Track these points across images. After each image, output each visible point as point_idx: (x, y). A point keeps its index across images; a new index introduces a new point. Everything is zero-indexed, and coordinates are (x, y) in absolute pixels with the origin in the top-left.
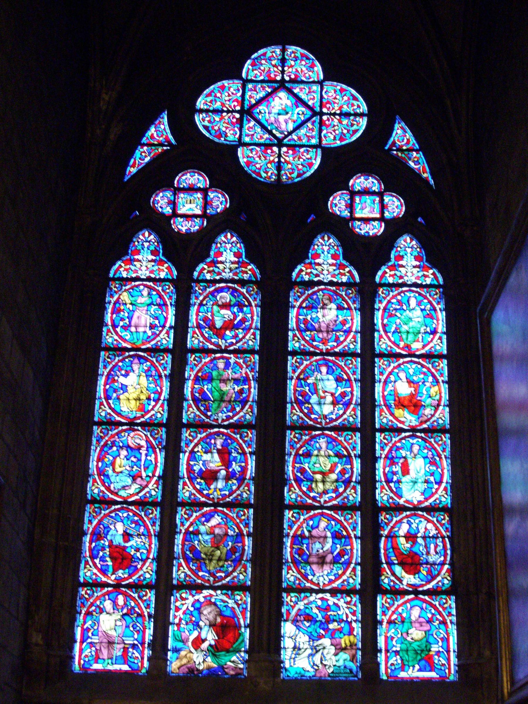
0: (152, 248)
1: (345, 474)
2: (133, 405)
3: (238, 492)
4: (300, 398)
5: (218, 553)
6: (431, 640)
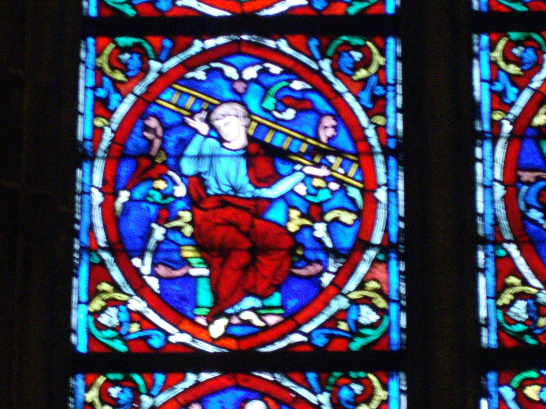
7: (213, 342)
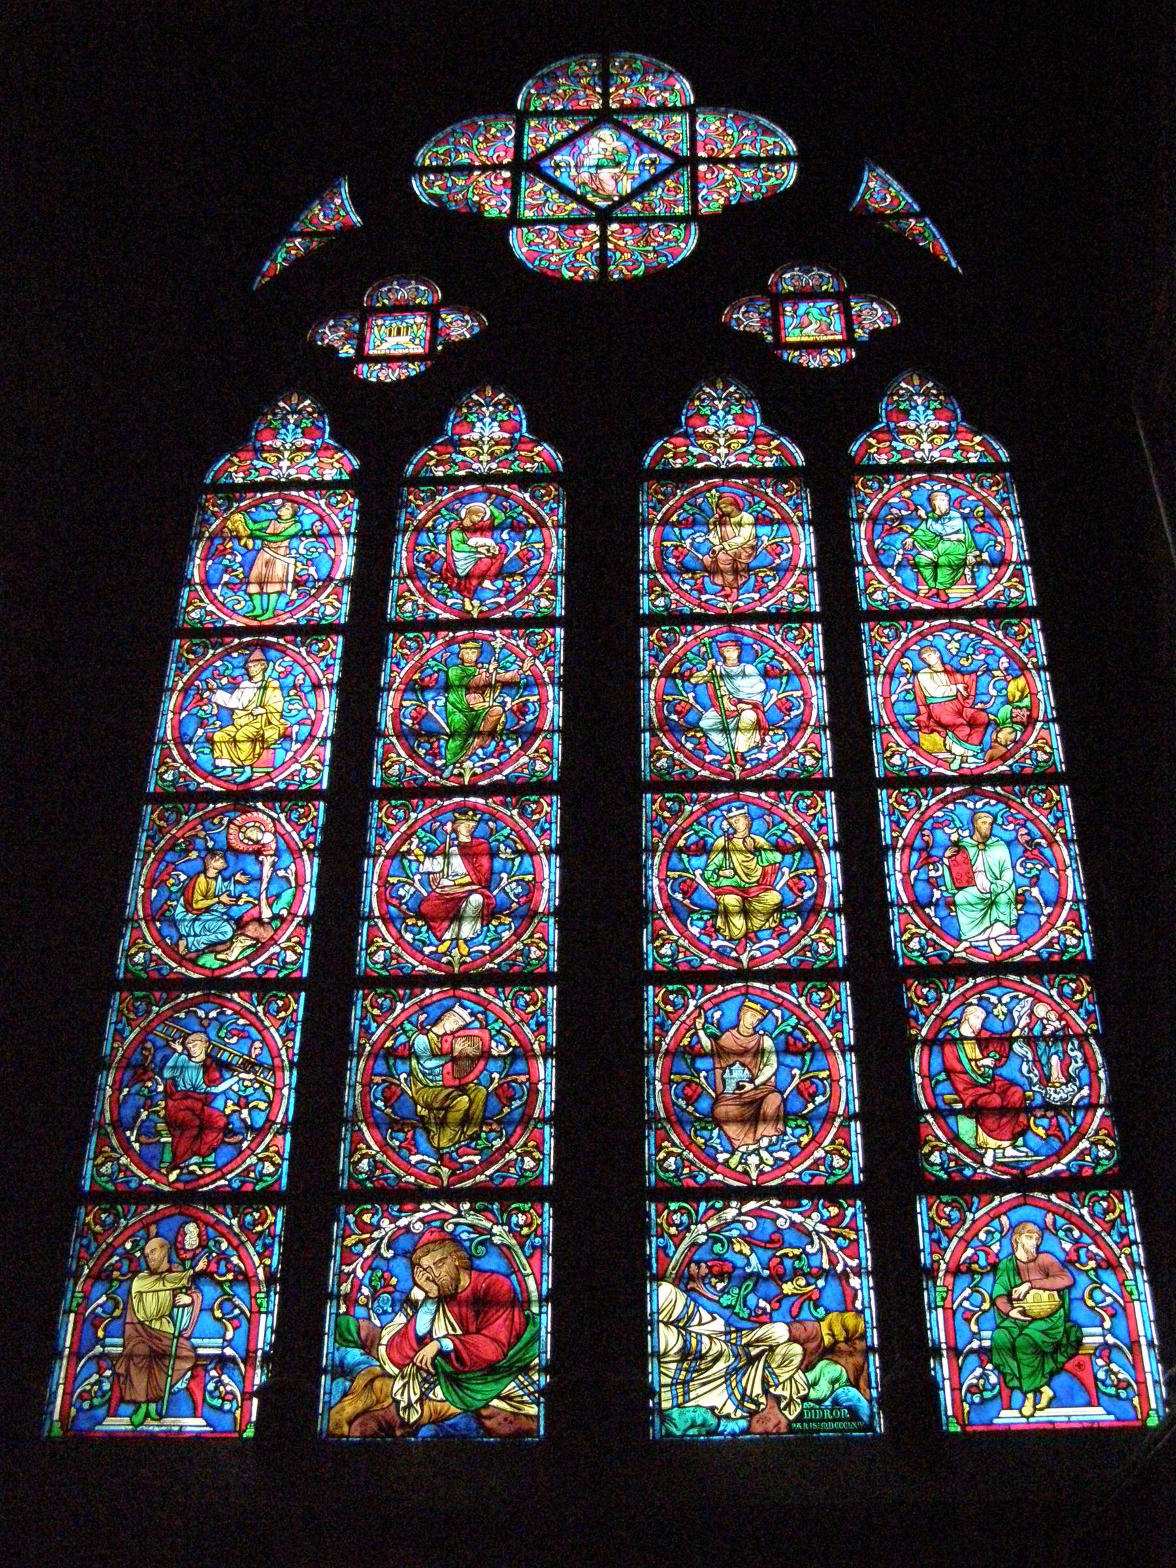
3: (519, 946)
4: (674, 717)
6: (1080, 1314)
7: (170, 1184)
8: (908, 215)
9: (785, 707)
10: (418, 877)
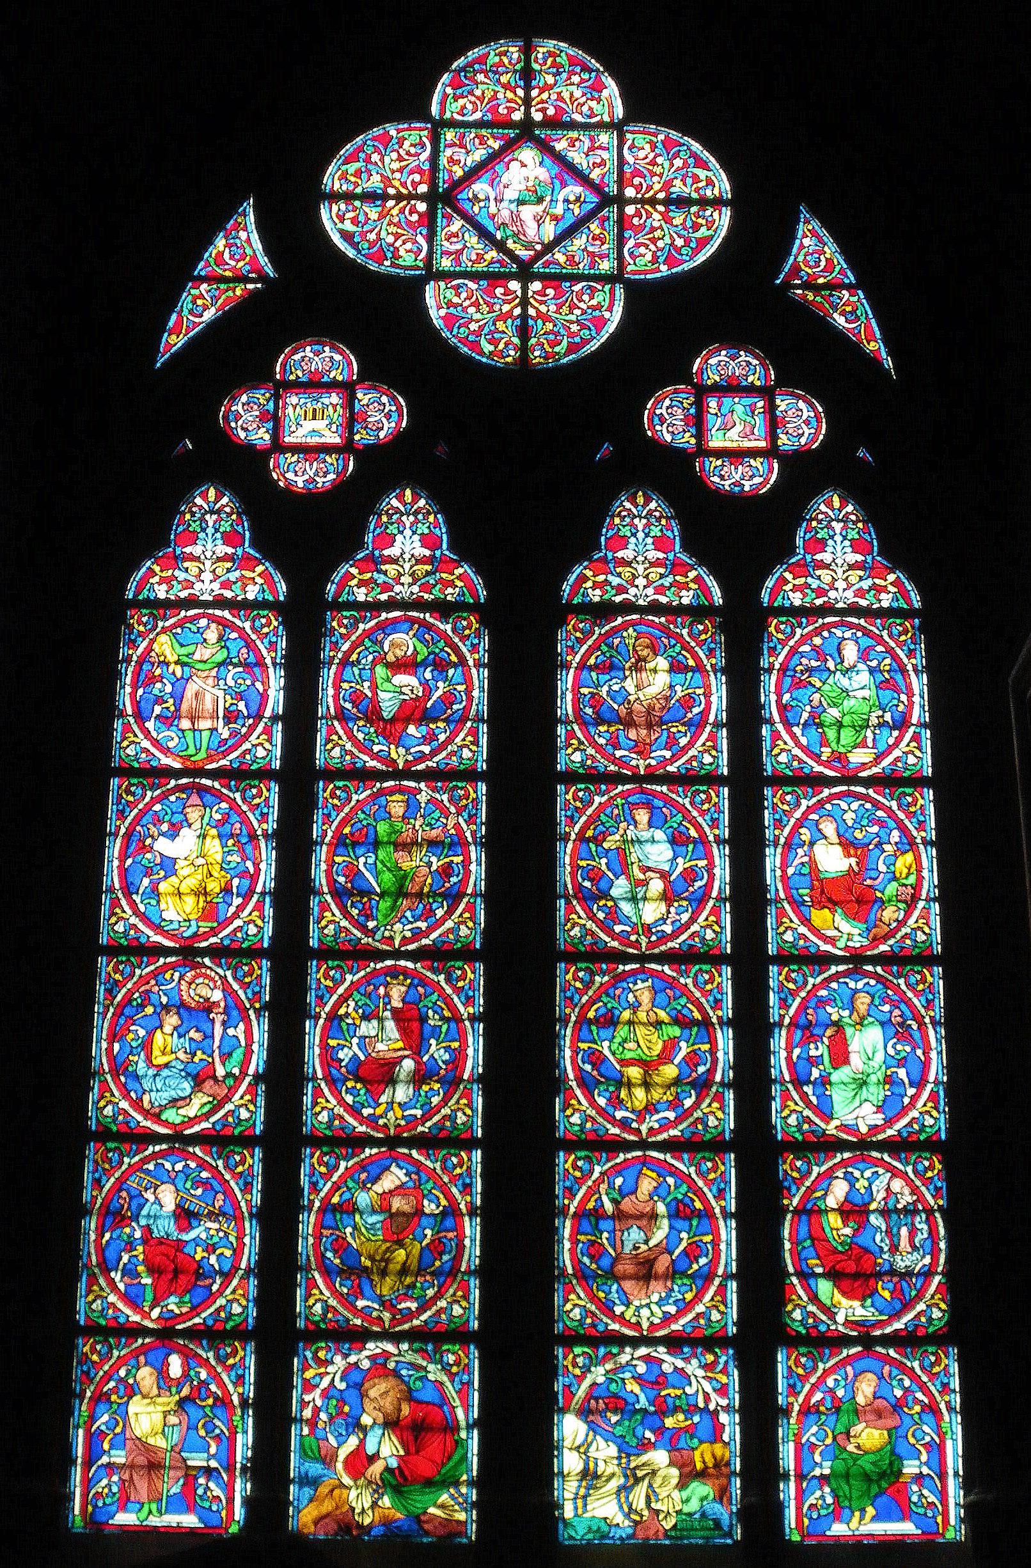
0: (225, 527)
1: (696, 1065)
2: (190, 904)
3: (446, 1111)
4: (587, 884)
5: (401, 1255)
6: (902, 1449)
8: (840, 286)
9: (690, 875)
10: (355, 1041)
